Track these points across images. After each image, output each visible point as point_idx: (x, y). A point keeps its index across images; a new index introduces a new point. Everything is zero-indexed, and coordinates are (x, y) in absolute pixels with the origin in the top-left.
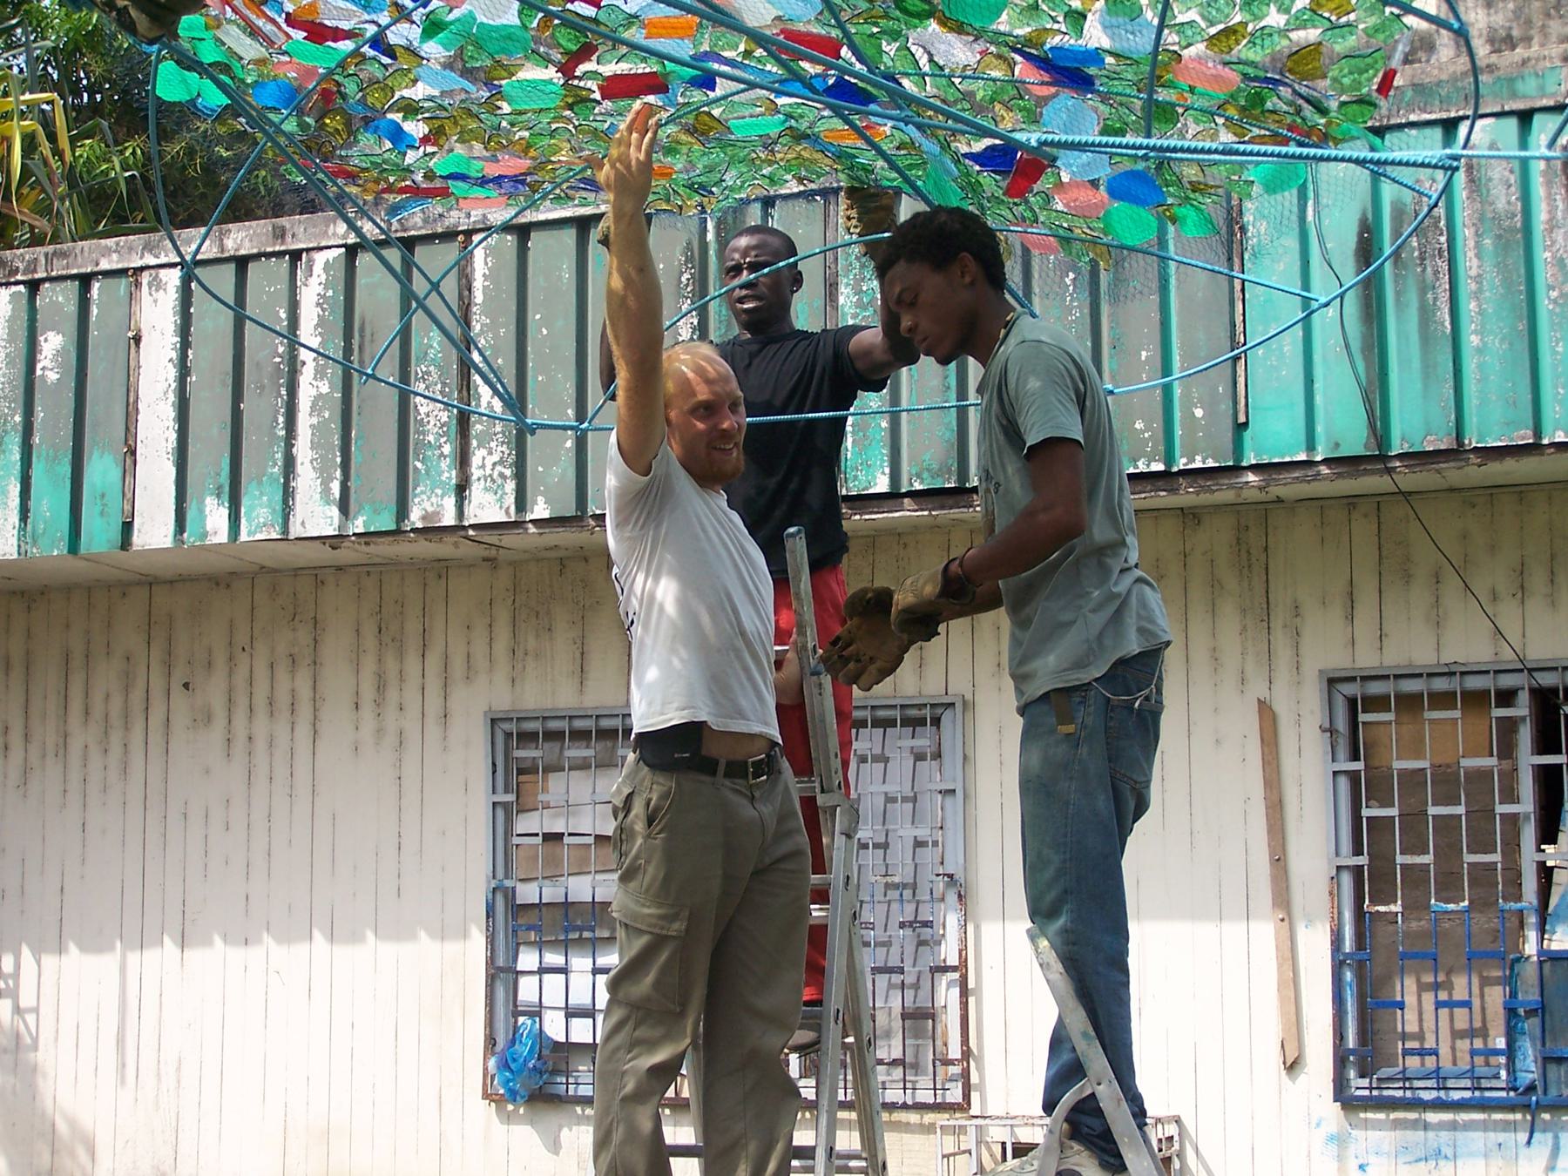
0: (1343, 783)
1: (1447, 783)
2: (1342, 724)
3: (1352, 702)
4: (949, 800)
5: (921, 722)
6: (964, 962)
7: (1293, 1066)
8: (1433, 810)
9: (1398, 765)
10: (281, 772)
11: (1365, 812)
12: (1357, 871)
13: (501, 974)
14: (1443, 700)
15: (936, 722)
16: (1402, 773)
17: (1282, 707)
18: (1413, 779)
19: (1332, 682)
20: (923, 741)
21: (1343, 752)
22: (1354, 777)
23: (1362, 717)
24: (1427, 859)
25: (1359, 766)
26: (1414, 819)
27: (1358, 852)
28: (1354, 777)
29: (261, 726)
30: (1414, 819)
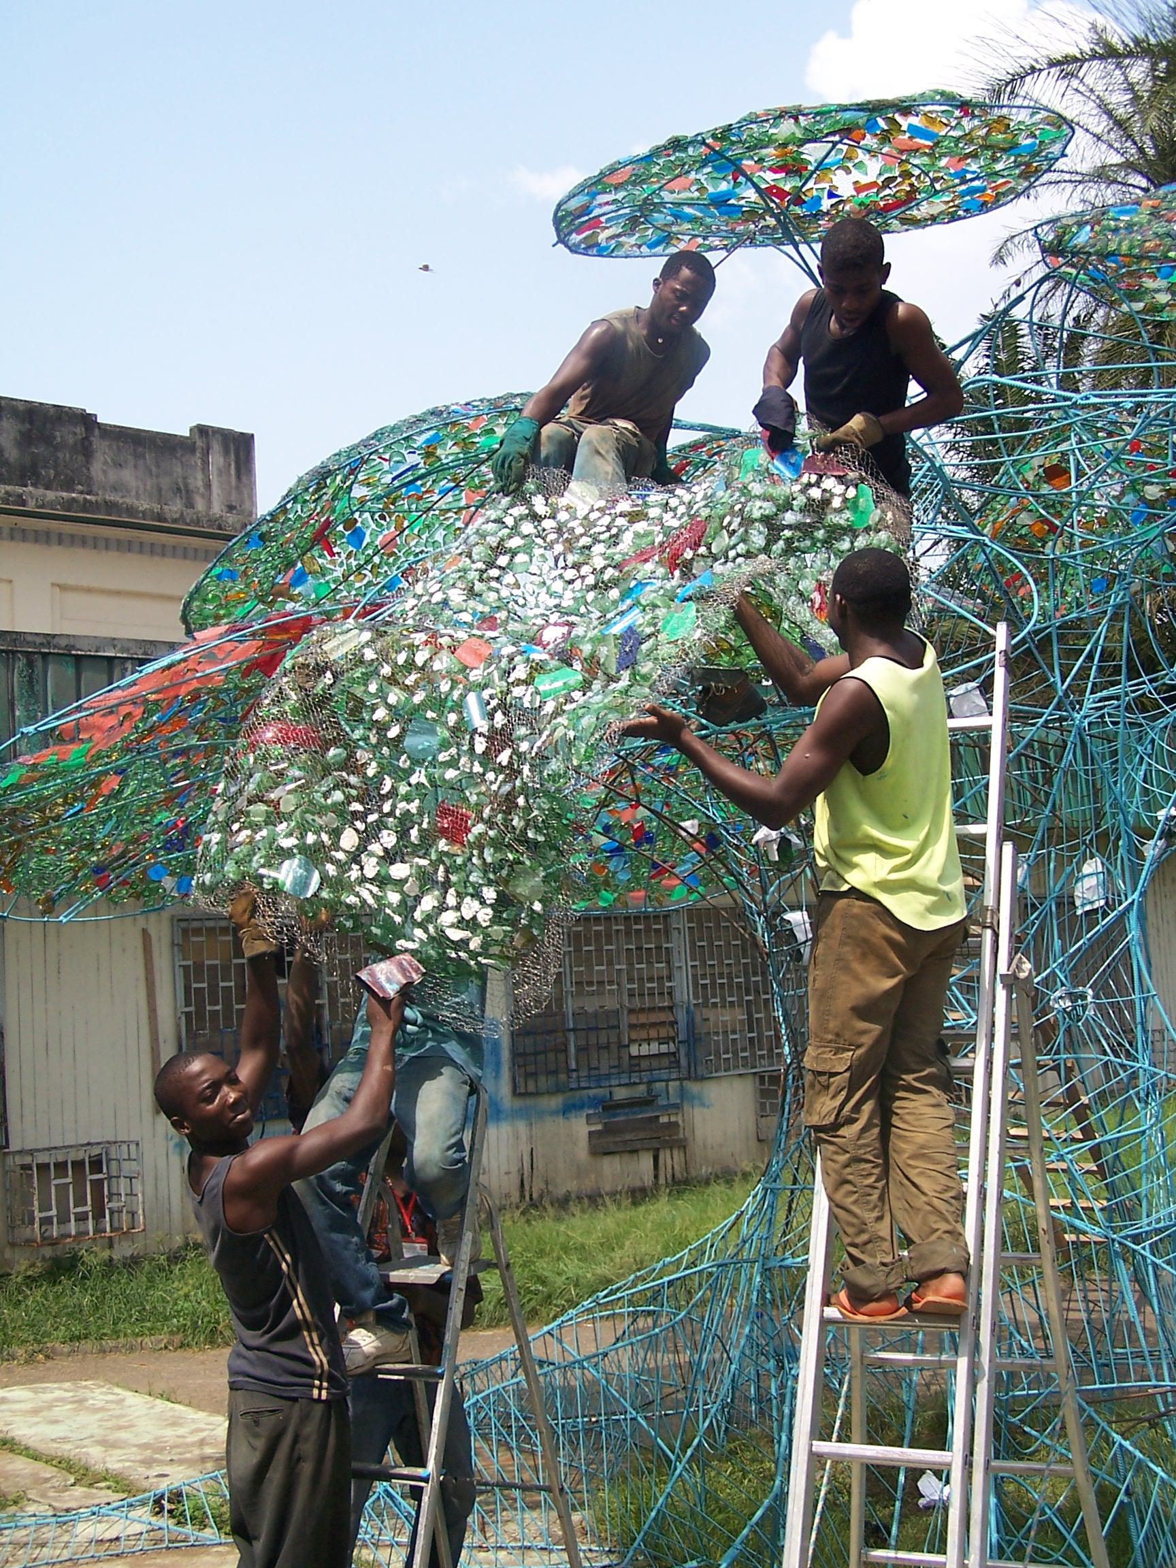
12: (188, 1015)
16: (209, 966)
17: (153, 932)
26: (213, 987)
27: (187, 1005)
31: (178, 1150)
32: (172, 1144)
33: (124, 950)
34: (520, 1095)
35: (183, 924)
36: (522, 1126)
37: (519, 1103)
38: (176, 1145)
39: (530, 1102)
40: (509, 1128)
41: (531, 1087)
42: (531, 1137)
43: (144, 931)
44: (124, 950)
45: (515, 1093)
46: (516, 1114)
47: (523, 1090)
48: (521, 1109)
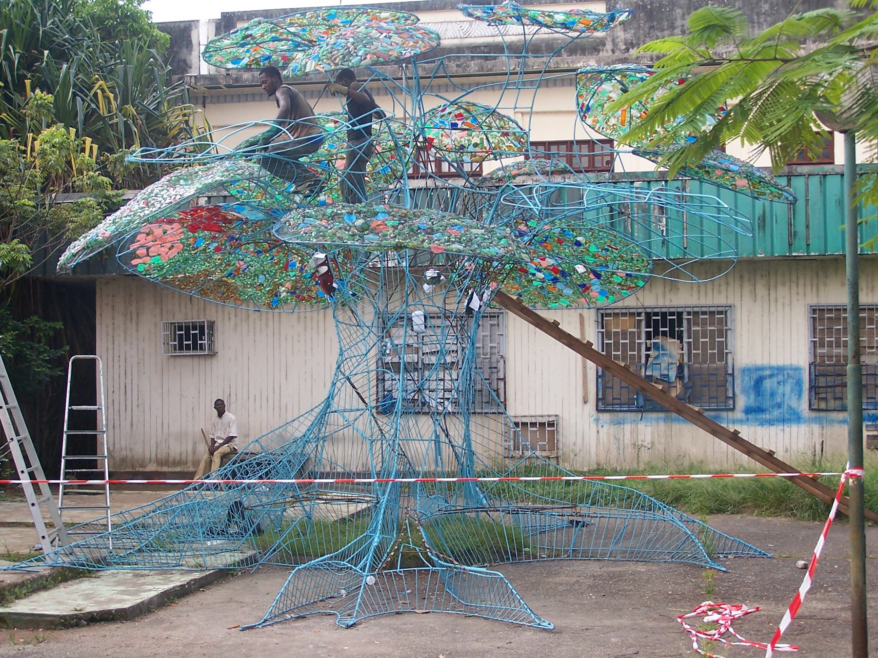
0: (600, 334)
1: (624, 334)
2: (600, 320)
3: (602, 315)
4: (501, 337)
5: (495, 317)
6: (505, 377)
7: (585, 402)
8: (621, 341)
9: (613, 330)
10: (315, 327)
11: (605, 342)
13: (381, 380)
14: (624, 314)
15: (498, 317)
16: (614, 332)
18: (616, 333)
19: (598, 309)
20: (495, 322)
21: (600, 326)
22: (602, 333)
23: (605, 318)
24: (620, 353)
25: (604, 330)
26: (616, 343)
28: (602, 333)
29: (308, 315)
30: (616, 343)
31: (595, 422)
32: (592, 419)
33: (569, 324)
34: (813, 410)
35: (601, 311)
36: (816, 428)
37: (814, 414)
38: (595, 420)
39: (822, 414)
40: (807, 428)
41: (823, 405)
42: (823, 435)
43: (581, 315)
44: (569, 324)
45: (811, 409)
46: (811, 421)
47: (816, 407)
48: (816, 418)
